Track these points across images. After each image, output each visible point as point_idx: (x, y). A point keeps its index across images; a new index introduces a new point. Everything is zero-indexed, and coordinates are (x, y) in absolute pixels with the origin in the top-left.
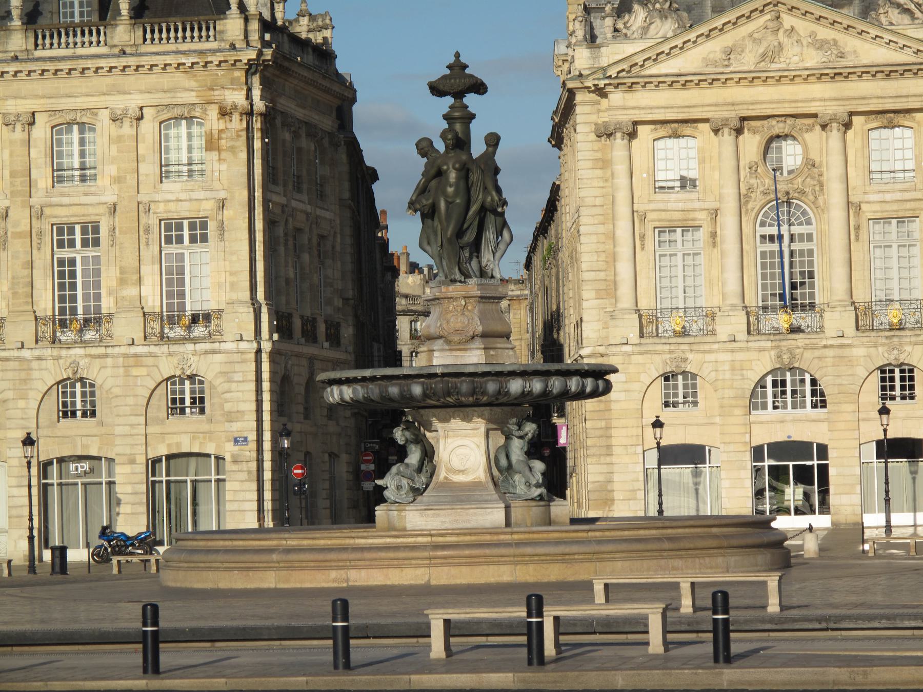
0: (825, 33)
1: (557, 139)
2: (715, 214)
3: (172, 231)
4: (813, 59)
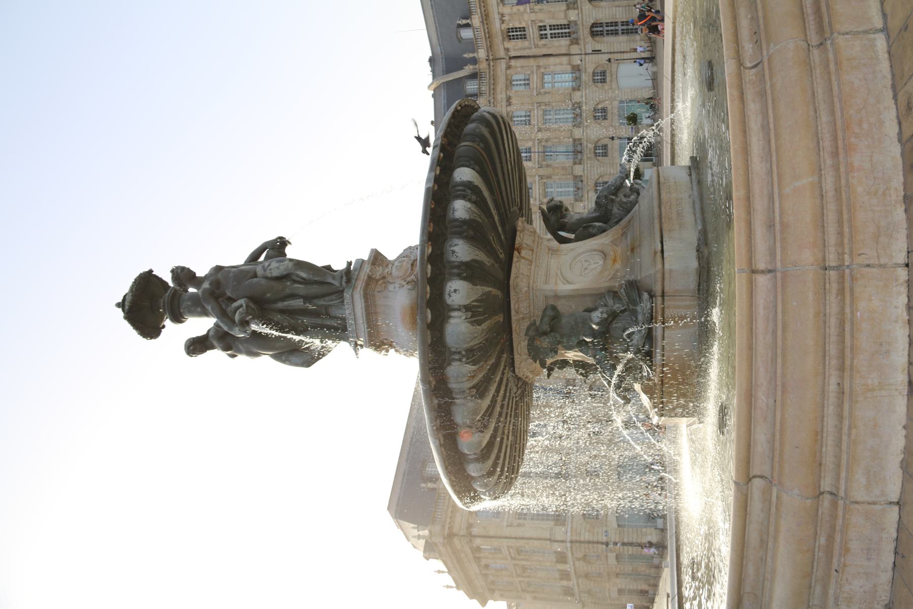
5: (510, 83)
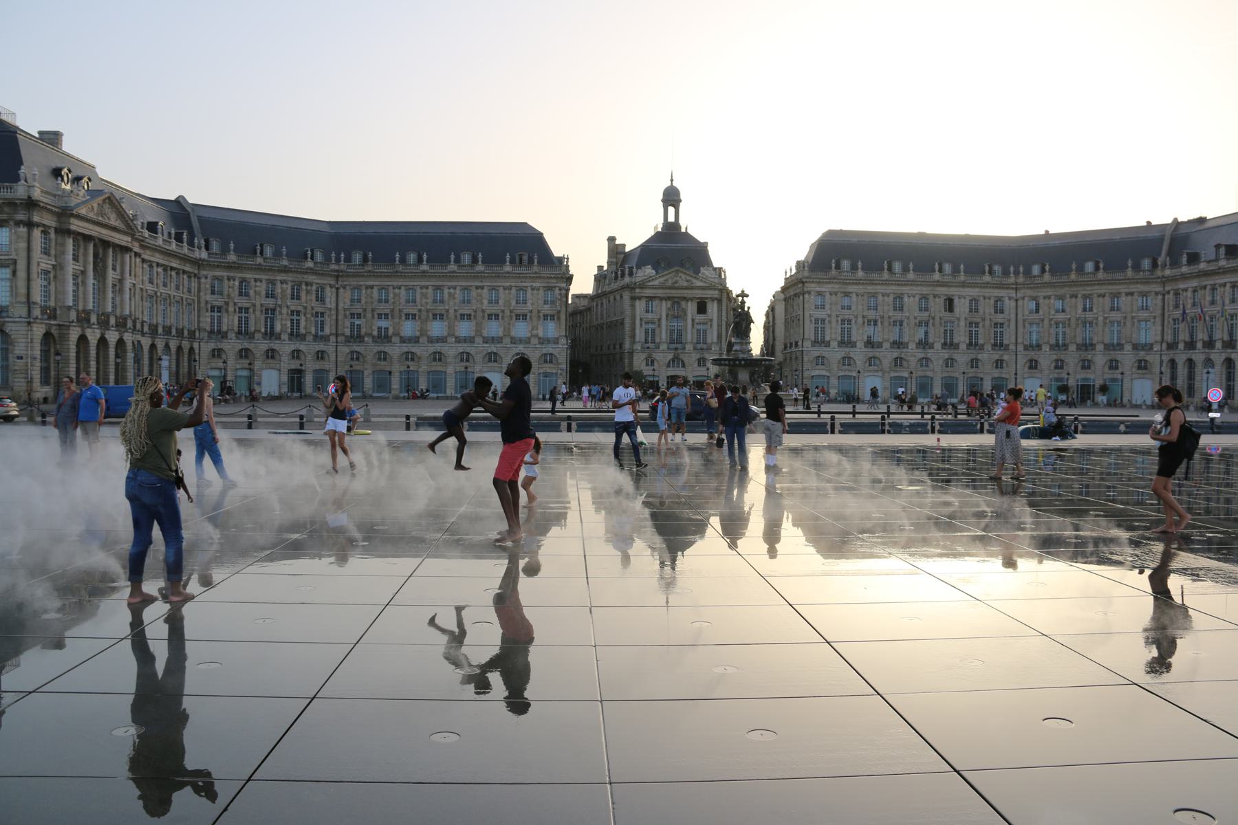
2: (660, 320)
3: (545, 316)
4: (685, 284)
5: (1144, 294)
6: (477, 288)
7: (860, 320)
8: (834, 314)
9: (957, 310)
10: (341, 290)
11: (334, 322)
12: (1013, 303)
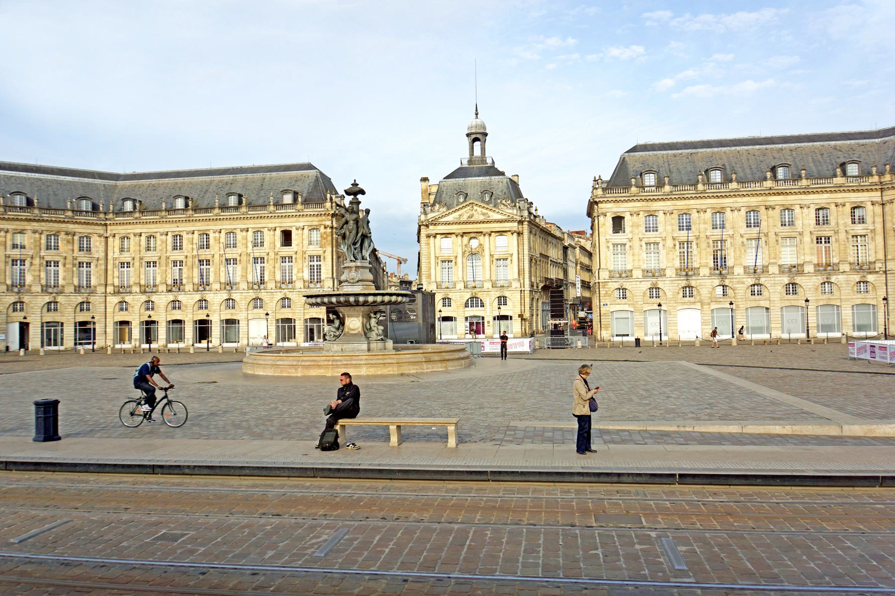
0: (485, 211)
1: (419, 241)
2: (456, 257)
4: (482, 218)
6: (242, 230)
7: (670, 243)
8: (636, 238)
9: (798, 223)
10: (110, 240)
11: (102, 273)
12: (878, 209)
